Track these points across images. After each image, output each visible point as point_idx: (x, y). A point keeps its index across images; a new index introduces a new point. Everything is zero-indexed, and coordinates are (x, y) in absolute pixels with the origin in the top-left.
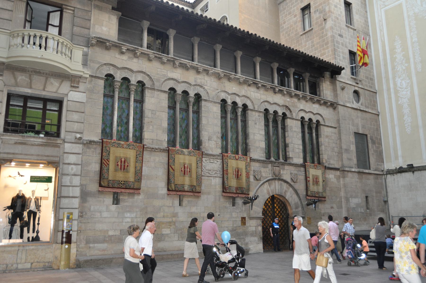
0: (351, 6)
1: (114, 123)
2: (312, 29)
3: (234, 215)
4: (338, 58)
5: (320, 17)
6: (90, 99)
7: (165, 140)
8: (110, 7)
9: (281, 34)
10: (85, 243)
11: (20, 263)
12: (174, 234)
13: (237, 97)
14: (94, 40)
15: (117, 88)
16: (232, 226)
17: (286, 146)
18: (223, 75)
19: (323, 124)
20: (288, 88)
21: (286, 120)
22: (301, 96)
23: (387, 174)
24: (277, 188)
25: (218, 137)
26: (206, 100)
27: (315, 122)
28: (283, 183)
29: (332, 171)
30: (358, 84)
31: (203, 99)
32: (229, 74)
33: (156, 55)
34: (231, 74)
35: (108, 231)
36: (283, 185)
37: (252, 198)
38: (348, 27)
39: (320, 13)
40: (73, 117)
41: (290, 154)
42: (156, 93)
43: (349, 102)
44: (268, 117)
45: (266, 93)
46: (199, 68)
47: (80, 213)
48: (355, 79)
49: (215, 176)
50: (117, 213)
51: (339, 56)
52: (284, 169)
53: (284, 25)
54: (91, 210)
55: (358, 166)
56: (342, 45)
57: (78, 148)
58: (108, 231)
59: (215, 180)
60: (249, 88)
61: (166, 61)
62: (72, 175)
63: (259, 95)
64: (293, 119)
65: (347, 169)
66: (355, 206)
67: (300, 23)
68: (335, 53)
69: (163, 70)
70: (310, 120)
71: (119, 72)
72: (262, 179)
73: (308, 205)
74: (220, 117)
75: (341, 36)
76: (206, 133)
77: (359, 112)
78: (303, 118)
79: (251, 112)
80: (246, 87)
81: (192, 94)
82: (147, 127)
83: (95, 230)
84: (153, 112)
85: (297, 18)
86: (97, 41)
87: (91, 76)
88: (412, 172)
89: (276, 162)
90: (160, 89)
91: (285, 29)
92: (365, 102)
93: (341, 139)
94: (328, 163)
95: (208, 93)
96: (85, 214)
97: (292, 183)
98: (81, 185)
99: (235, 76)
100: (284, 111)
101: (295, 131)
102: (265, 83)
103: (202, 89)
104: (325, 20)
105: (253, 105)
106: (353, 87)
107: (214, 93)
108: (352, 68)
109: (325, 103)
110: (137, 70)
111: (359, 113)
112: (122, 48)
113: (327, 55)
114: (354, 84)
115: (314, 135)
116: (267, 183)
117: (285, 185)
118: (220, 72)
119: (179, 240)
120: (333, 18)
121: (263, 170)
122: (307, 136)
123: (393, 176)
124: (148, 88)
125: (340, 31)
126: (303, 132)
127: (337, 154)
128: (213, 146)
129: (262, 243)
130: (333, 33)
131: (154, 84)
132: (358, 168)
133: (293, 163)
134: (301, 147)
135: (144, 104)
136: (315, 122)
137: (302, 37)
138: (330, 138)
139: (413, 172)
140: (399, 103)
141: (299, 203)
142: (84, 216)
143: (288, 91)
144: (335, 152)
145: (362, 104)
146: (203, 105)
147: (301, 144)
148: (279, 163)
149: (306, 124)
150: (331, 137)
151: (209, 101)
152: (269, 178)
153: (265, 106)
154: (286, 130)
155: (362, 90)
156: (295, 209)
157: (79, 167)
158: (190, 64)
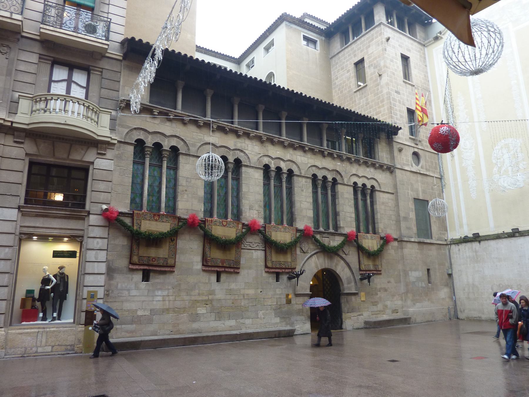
0: (409, 60)
1: (145, 193)
2: (367, 85)
3: (278, 291)
4: (395, 116)
5: (374, 72)
6: (118, 166)
9: (334, 91)
11: (40, 346)
13: (282, 162)
15: (148, 154)
17: (336, 214)
18: (266, 138)
19: (379, 189)
20: (339, 151)
21: (336, 186)
22: (353, 160)
23: (451, 244)
25: (260, 206)
26: (246, 166)
30: (417, 145)
31: (244, 165)
32: (273, 137)
35: (136, 310)
37: (297, 273)
38: (406, 83)
39: (374, 68)
40: (99, 186)
41: (342, 224)
43: (408, 165)
44: (317, 183)
45: (313, 156)
47: (106, 292)
48: (414, 140)
50: (147, 290)
51: (396, 115)
53: (336, 81)
54: (118, 288)
55: (418, 235)
56: (400, 102)
58: (136, 310)
59: (256, 253)
61: (202, 124)
63: (306, 159)
65: (405, 239)
66: (415, 281)
67: (354, 78)
68: (391, 111)
69: (199, 134)
70: (364, 185)
71: (150, 137)
72: (309, 252)
73: (361, 279)
75: (397, 92)
77: (419, 175)
78: (355, 183)
80: (291, 151)
83: (122, 309)
85: (350, 73)
87: (119, 142)
88: (478, 242)
90: (196, 155)
91: (338, 85)
92: (425, 164)
93: (399, 205)
95: (249, 158)
96: (111, 292)
98: (107, 261)
101: (347, 198)
102: (313, 146)
103: (242, 154)
104: (380, 75)
105: (300, 170)
106: (412, 148)
107: (256, 158)
108: (411, 128)
109: (381, 167)
110: (170, 134)
111: (420, 178)
113: (382, 113)
114: (413, 145)
115: (369, 201)
116: (315, 256)
118: (262, 135)
119: (215, 320)
120: (389, 74)
122: (360, 203)
123: (457, 246)
124: (183, 154)
125: (397, 87)
127: (394, 222)
130: (389, 90)
131: (189, 149)
132: (418, 237)
133: (344, 233)
134: (353, 215)
135: (178, 171)
137: (355, 94)
138: (387, 205)
139: (480, 242)
140: (463, 165)
141: (352, 277)
142: (110, 295)
143: (338, 154)
145: (422, 167)
146: (243, 170)
147: (354, 212)
148: (328, 233)
149: (359, 190)
150: (387, 204)
151: (250, 166)
153: (313, 171)
155: (422, 151)
156: (347, 285)
157: (106, 240)
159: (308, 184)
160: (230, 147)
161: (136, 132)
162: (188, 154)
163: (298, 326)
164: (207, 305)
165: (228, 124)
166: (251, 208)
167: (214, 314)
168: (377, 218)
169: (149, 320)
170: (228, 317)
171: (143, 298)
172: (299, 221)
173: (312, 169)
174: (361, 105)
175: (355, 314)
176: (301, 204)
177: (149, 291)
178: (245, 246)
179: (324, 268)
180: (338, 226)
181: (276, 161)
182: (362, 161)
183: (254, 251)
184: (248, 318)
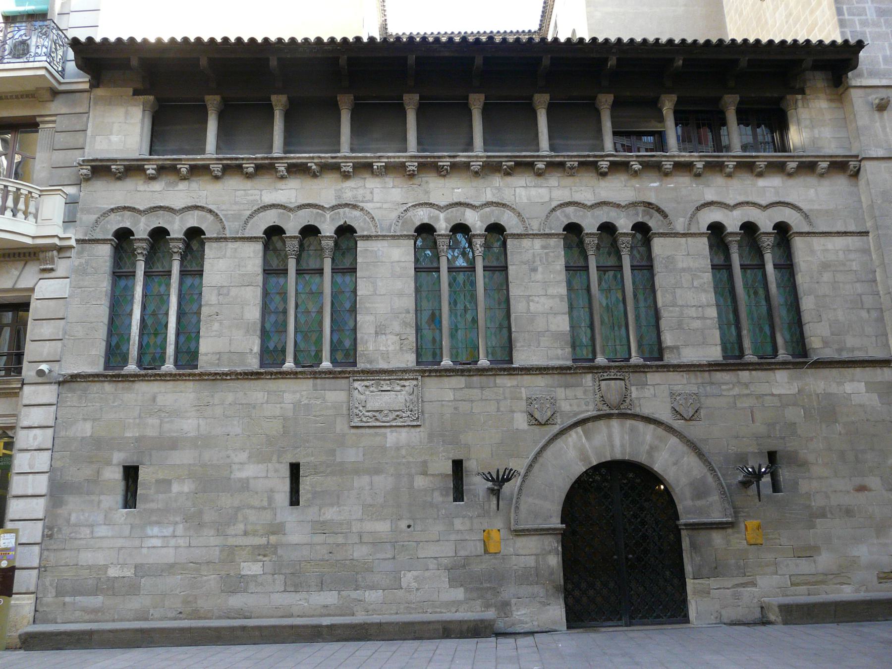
3: (458, 524)
8: (130, 91)
10: (54, 594)
12: (273, 575)
14: (84, 167)
16: (452, 554)
19: (806, 229)
24: (617, 442)
25: (405, 324)
26: (368, 238)
28: (640, 425)
29: (858, 371)
31: (360, 237)
32: (434, 157)
33: (225, 162)
34: (439, 157)
35: (106, 567)
40: (42, 330)
41: (668, 339)
42: (231, 245)
45: (568, 181)
50: (129, 526)
54: (71, 522)
57: (48, 393)
58: (106, 567)
59: (394, 434)
60: (509, 180)
62: (35, 450)
63: (543, 192)
64: (676, 235)
70: (749, 228)
71: (143, 219)
74: (413, 271)
79: (516, 241)
80: (497, 181)
81: (328, 229)
82: (207, 328)
83: (77, 565)
84: (220, 290)
86: (92, 167)
90: (239, 235)
94: (836, 346)
95: (373, 218)
96: (57, 531)
97: (678, 424)
98: (52, 470)
100: (640, 220)
103: (357, 213)
107: (394, 215)
109: (808, 167)
110: (183, 206)
112: (146, 167)
116: (579, 429)
117: (648, 433)
118: (404, 160)
119: (285, 591)
121: (561, 393)
128: (391, 348)
129: (562, 602)
138: (842, 268)
141: (710, 479)
142: (56, 536)
143: (646, 159)
144: (868, 311)
147: (713, 300)
150: (844, 265)
153: (567, 216)
156: (692, 500)
157: (50, 432)
158: (316, 161)
159: (553, 252)
160: (321, 204)
161: (116, 215)
162: (221, 238)
163: (523, 612)
164: (265, 556)
165: (311, 155)
166: (380, 331)
167: (282, 577)
169: (132, 589)
170: (317, 586)
171: (120, 543)
172: (522, 346)
174: (778, 25)
175: (729, 582)
176: (531, 304)
177: (132, 527)
178: (361, 421)
179: (609, 459)
180: (664, 345)
181: (452, 212)
182: (731, 165)
183: (388, 430)
184: (372, 588)
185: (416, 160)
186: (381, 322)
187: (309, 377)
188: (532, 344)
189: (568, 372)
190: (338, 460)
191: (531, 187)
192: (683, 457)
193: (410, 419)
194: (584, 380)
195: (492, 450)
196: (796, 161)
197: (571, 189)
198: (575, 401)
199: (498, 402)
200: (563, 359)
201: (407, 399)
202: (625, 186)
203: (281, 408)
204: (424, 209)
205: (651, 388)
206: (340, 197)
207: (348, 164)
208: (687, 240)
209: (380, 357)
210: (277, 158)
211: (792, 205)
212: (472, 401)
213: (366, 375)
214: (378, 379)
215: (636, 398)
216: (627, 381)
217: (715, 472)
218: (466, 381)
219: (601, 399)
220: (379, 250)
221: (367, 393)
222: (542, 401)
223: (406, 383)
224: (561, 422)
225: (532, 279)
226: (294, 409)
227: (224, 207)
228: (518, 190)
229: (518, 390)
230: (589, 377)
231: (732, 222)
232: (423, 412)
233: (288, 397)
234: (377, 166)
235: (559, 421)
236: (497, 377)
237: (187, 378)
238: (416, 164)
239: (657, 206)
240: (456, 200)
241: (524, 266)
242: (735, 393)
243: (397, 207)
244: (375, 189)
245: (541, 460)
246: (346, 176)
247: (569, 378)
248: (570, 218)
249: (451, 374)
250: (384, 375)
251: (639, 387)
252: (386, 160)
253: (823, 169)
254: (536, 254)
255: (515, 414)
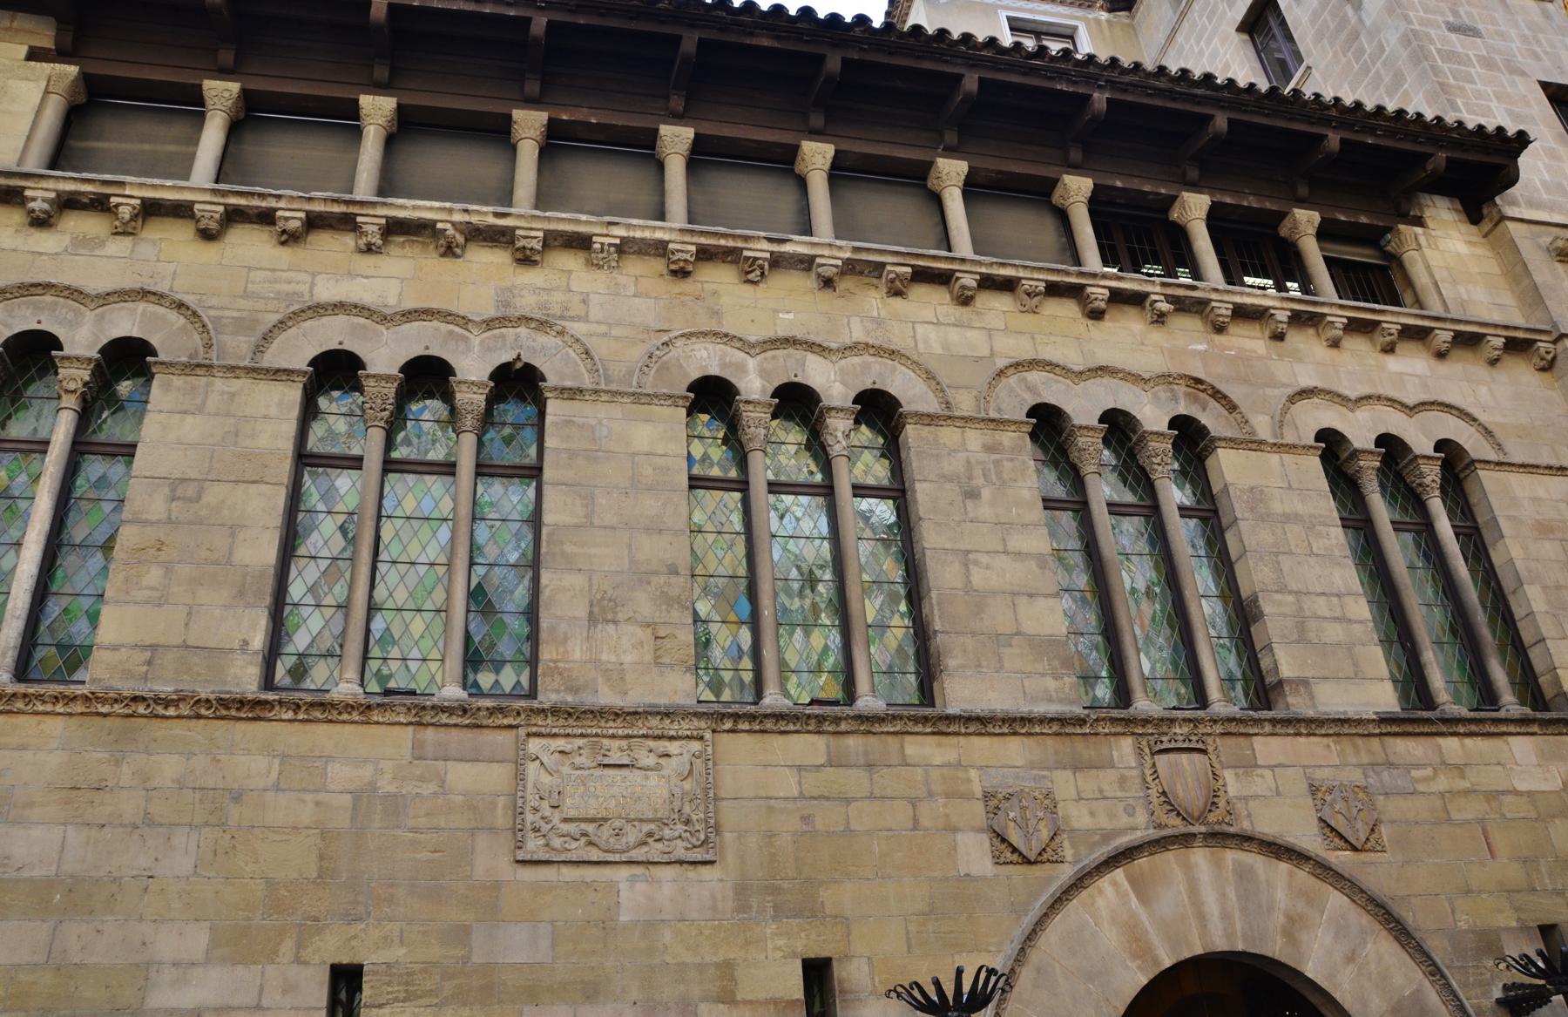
2: (1309, 68)
7: (246, 643)
21: (1210, 463)
26: (572, 393)
27: (1430, 451)
34: (746, 238)
36: (1262, 876)
41: (1286, 662)
42: (219, 384)
44: (1074, 456)
46: (518, 232)
49: (638, 854)
52: (1249, 765)
56: (1488, 64)
64: (1256, 445)
70: (1390, 445)
76: (577, 581)
79: (926, 431)
82: (127, 580)
89: (1172, 721)
97: (1341, 859)
99: (775, 248)
100: (1182, 409)
103: (547, 340)
105: (939, 389)
107: (637, 353)
109: (1468, 341)
112: (28, 193)
115: (1444, 526)
116: (1119, 874)
118: (666, 237)
121: (1064, 784)
122: (1398, 550)
125: (1455, 13)
126: (1358, 522)
130: (1410, 22)
134: (1361, 609)
136: (1430, 451)
141: (1433, 997)
143: (1181, 292)
152: (1124, 841)
153: (1031, 389)
154: (1224, 521)
158: (457, 217)
166: (601, 613)
168: (1531, 614)
173: (1024, 380)
179: (1199, 951)
180: (1269, 680)
181: (774, 357)
183: (624, 872)
185: (696, 239)
186: (605, 592)
187: (402, 720)
188: (984, 664)
189: (1078, 730)
190: (477, 959)
191: (948, 324)
192: (1366, 943)
193: (685, 844)
194: (1115, 753)
195: (908, 932)
196: (1450, 330)
197: (1033, 338)
198: (1105, 801)
199: (914, 802)
200: (1061, 701)
201: (677, 792)
202: (1143, 344)
203: (318, 804)
204: (710, 346)
205: (1268, 773)
206: (507, 305)
207: (533, 234)
208: (1281, 458)
209: (600, 680)
210: (362, 203)
211: (1457, 409)
212: (848, 801)
213: (561, 722)
214: (597, 735)
215: (1239, 798)
216: (1213, 757)
217: (1443, 976)
218: (828, 747)
219: (1162, 799)
220: (600, 423)
221: (566, 770)
222: (1025, 803)
223: (673, 747)
224: (1074, 855)
225: (971, 515)
226: (355, 808)
227: (214, 302)
228: (918, 327)
229: (961, 774)
230: (1127, 744)
231: (1361, 430)
232: (717, 829)
233: (341, 774)
234: (602, 244)
235: (1068, 853)
236: (908, 738)
237: (49, 708)
238: (693, 248)
239: (1213, 388)
240: (781, 333)
241: (948, 486)
242: (1441, 788)
243: (646, 336)
244: (591, 296)
245: (1034, 956)
246: (526, 259)
247: (1079, 744)
248: (1039, 395)
249: (791, 727)
250: (611, 724)
251: (1241, 771)
252: (621, 232)
253: (1496, 349)
254: (973, 460)
255: (959, 836)
